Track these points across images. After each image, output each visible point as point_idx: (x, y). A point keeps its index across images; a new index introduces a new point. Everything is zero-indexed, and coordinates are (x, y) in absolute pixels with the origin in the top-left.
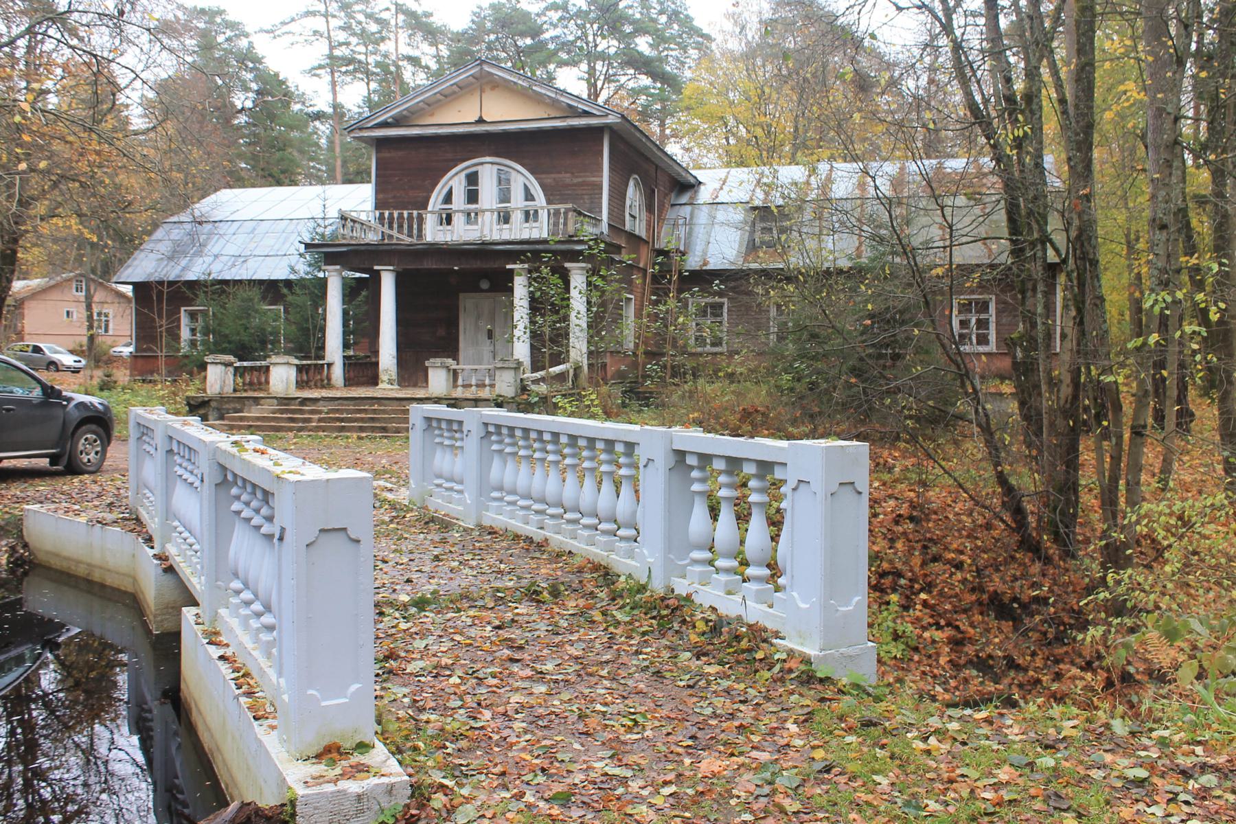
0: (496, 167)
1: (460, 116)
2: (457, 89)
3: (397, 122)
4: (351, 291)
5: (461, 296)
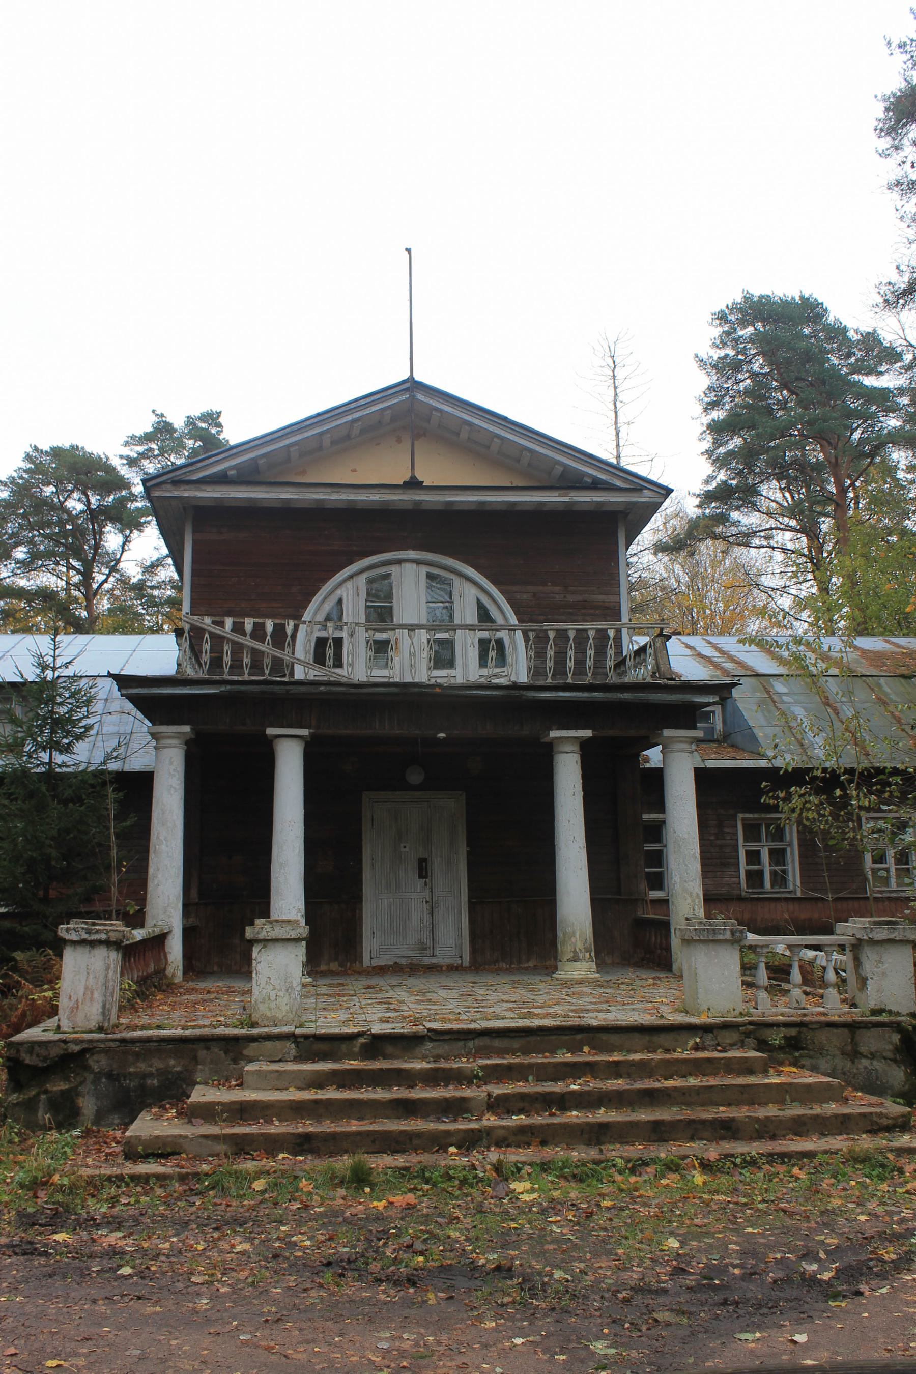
0: (424, 570)
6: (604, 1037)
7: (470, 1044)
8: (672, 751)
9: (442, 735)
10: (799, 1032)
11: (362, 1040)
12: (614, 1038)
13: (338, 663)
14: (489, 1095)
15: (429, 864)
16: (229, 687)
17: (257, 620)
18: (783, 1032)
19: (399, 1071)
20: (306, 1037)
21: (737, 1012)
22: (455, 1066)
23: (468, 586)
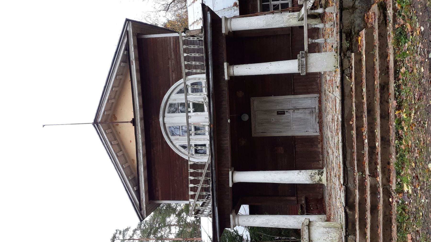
0: (166, 114)
3: (136, 183)
5: (254, 135)
6: (346, 115)
7: (349, 169)
8: (231, 28)
9: (229, 121)
10: (344, 33)
11: (348, 210)
12: (346, 111)
13: (204, 145)
14: (369, 176)
15: (279, 110)
16: (215, 203)
17: (189, 190)
18: (344, 42)
19: (360, 204)
20: (346, 231)
21: (336, 54)
22: (358, 182)
23: (171, 97)
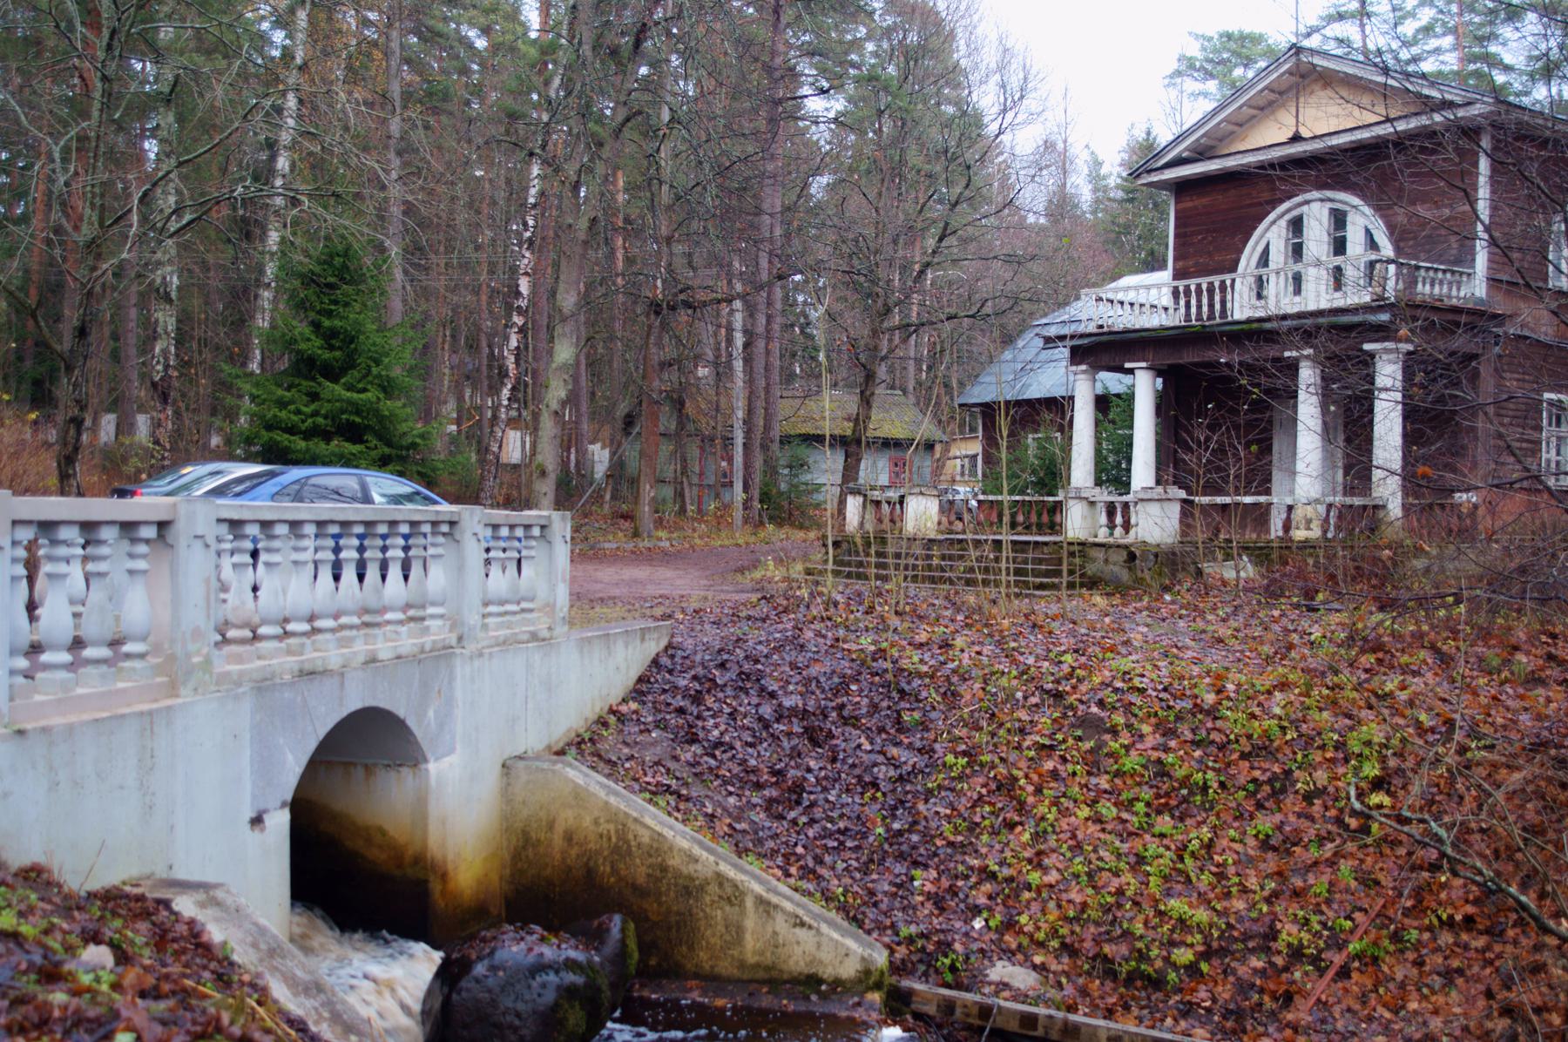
0: (1329, 205)
1: (1269, 137)
2: (1273, 96)
4: (1103, 403)
